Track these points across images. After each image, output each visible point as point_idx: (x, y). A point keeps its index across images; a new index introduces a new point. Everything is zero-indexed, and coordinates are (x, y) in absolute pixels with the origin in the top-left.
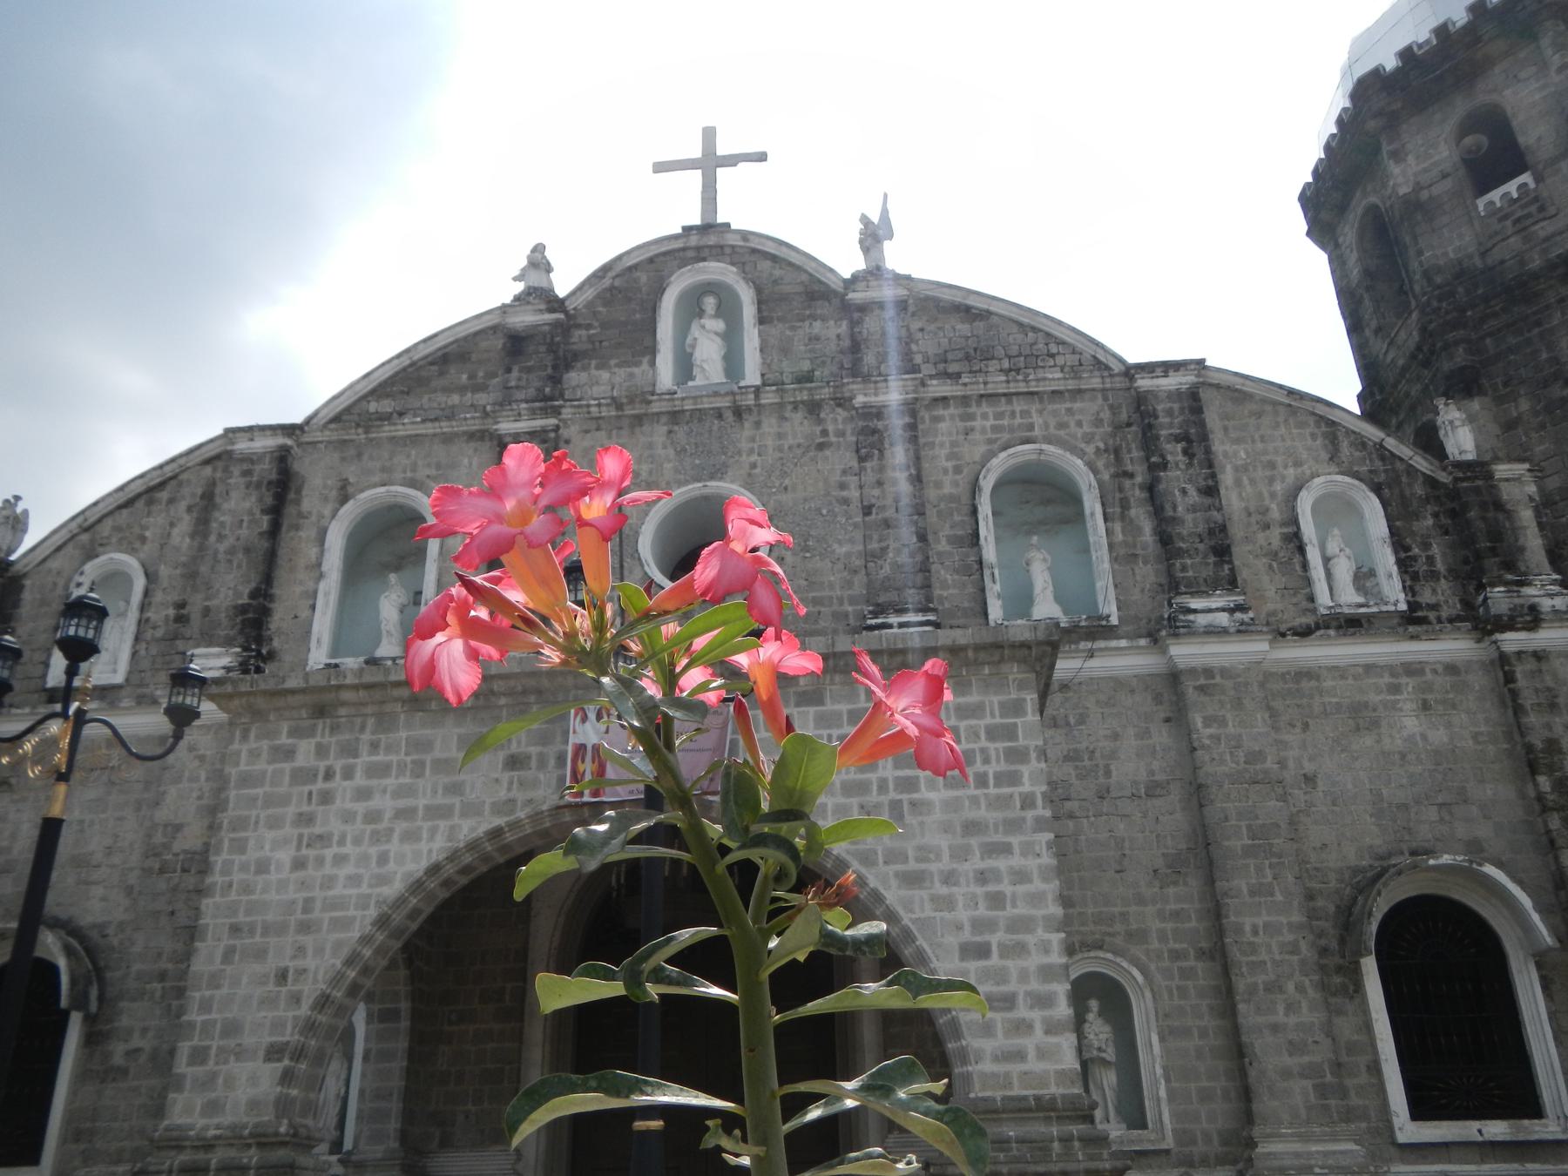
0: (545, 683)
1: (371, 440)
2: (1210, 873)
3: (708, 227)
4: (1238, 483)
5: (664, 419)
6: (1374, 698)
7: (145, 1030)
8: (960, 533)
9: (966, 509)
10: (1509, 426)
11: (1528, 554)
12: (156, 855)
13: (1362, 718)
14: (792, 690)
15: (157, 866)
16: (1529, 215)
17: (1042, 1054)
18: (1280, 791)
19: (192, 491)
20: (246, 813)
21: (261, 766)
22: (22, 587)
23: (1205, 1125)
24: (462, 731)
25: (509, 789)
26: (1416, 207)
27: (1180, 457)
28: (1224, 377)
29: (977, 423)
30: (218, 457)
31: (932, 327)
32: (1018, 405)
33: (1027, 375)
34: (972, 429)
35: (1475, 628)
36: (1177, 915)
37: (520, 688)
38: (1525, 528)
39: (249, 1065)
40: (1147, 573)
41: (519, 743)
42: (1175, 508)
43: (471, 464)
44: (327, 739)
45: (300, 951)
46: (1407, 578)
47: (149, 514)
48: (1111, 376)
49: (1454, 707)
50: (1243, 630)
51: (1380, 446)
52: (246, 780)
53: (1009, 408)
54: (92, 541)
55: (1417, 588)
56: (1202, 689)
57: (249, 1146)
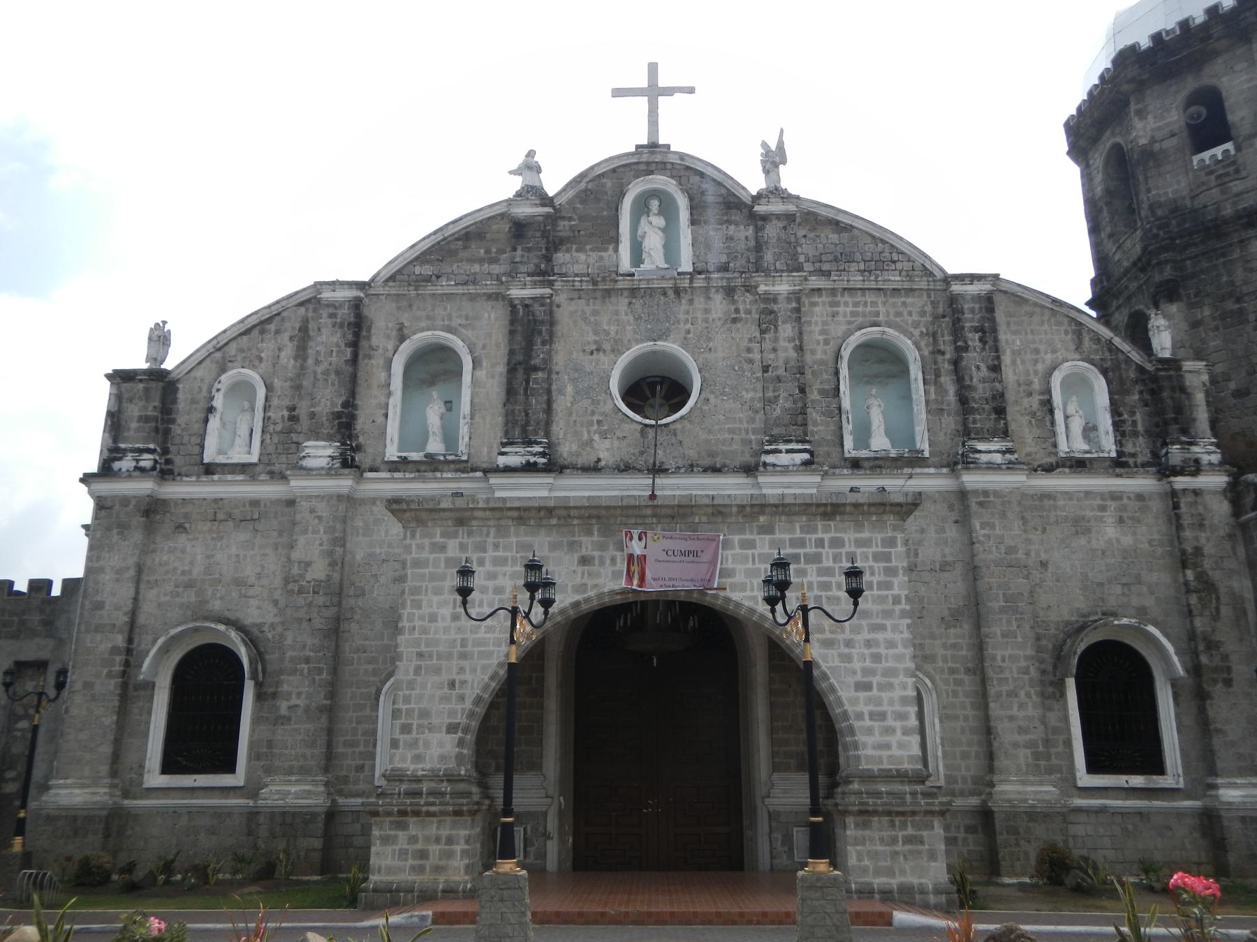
0: (603, 512)
1: (418, 295)
2: (978, 622)
3: (653, 146)
4: (1014, 363)
5: (626, 293)
6: (1089, 513)
7: (299, 694)
8: (827, 387)
9: (831, 370)
10: (1195, 325)
11: (1197, 424)
12: (295, 581)
13: (1080, 526)
14: (755, 524)
15: (296, 589)
16: (1227, 174)
17: (901, 746)
18: (1026, 573)
19: (292, 326)
20: (419, 584)
21: (425, 555)
22: (177, 389)
23: (963, 773)
24: (551, 539)
25: (582, 577)
26: (1150, 155)
27: (977, 343)
28: (1009, 286)
29: (841, 309)
30: (309, 301)
31: (812, 235)
32: (870, 298)
33: (877, 276)
34: (837, 313)
35: (1159, 472)
36: (954, 646)
37: (587, 515)
38: (1198, 405)
39: (437, 735)
40: (950, 423)
41: (587, 548)
42: (971, 379)
43: (489, 317)
44: (465, 540)
45: (462, 670)
46: (1118, 434)
47: (262, 341)
48: (934, 281)
49: (1139, 521)
50: (1011, 466)
51: (1110, 342)
52: (417, 563)
53: (863, 299)
54: (223, 358)
55: (1124, 442)
56: (981, 504)
57: (442, 781)
